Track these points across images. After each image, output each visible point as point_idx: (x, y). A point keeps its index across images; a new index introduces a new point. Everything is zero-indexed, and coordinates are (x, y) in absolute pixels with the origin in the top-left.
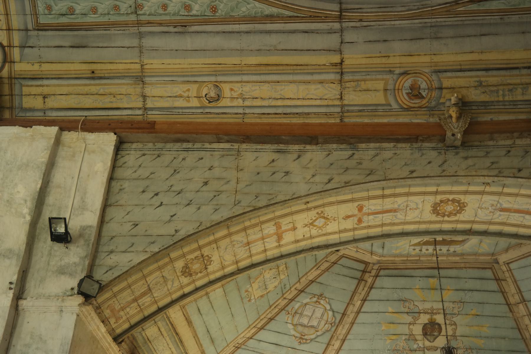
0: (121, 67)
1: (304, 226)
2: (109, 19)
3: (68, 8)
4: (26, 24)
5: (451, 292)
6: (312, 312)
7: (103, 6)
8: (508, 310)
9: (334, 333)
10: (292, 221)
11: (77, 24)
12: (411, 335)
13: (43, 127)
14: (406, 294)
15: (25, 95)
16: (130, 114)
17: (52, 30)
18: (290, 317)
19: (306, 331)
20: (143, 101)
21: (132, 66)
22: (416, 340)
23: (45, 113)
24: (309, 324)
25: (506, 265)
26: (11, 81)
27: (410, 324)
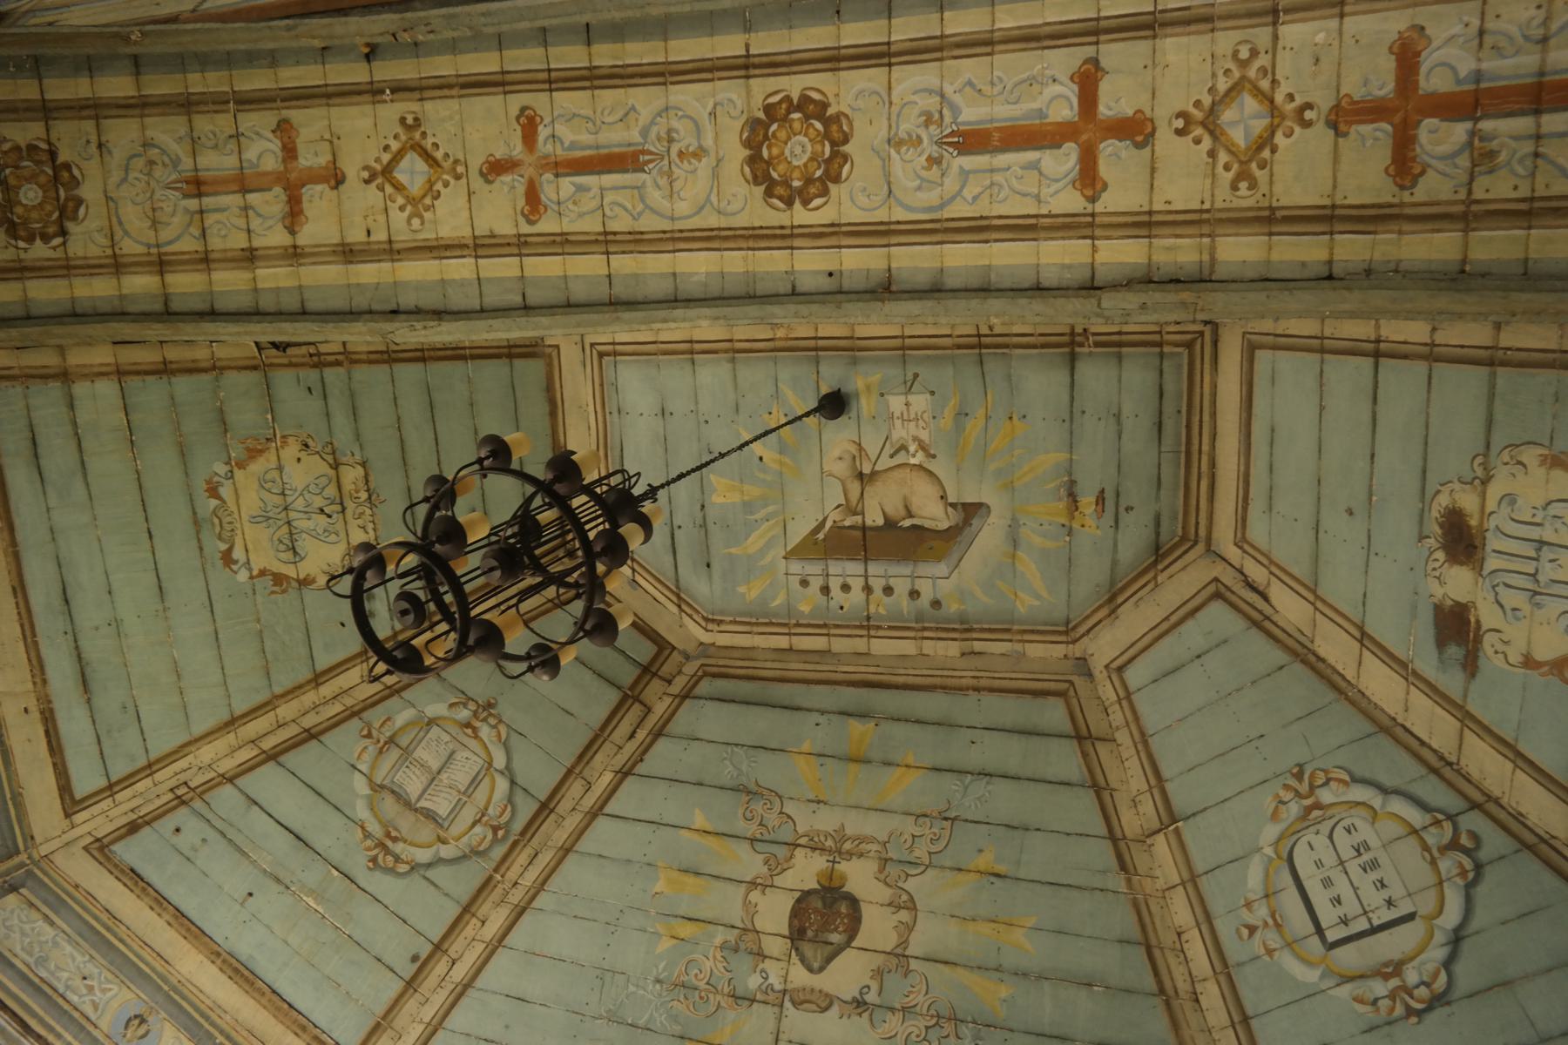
1: (366, 175)
5: (914, 775)
6: (444, 759)
8: (1114, 863)
9: (496, 870)
10: (327, 136)
12: (750, 930)
14: (766, 771)
18: (370, 748)
19: (406, 824)
22: (761, 955)
24: (423, 804)
25: (1115, 677)
27: (753, 884)
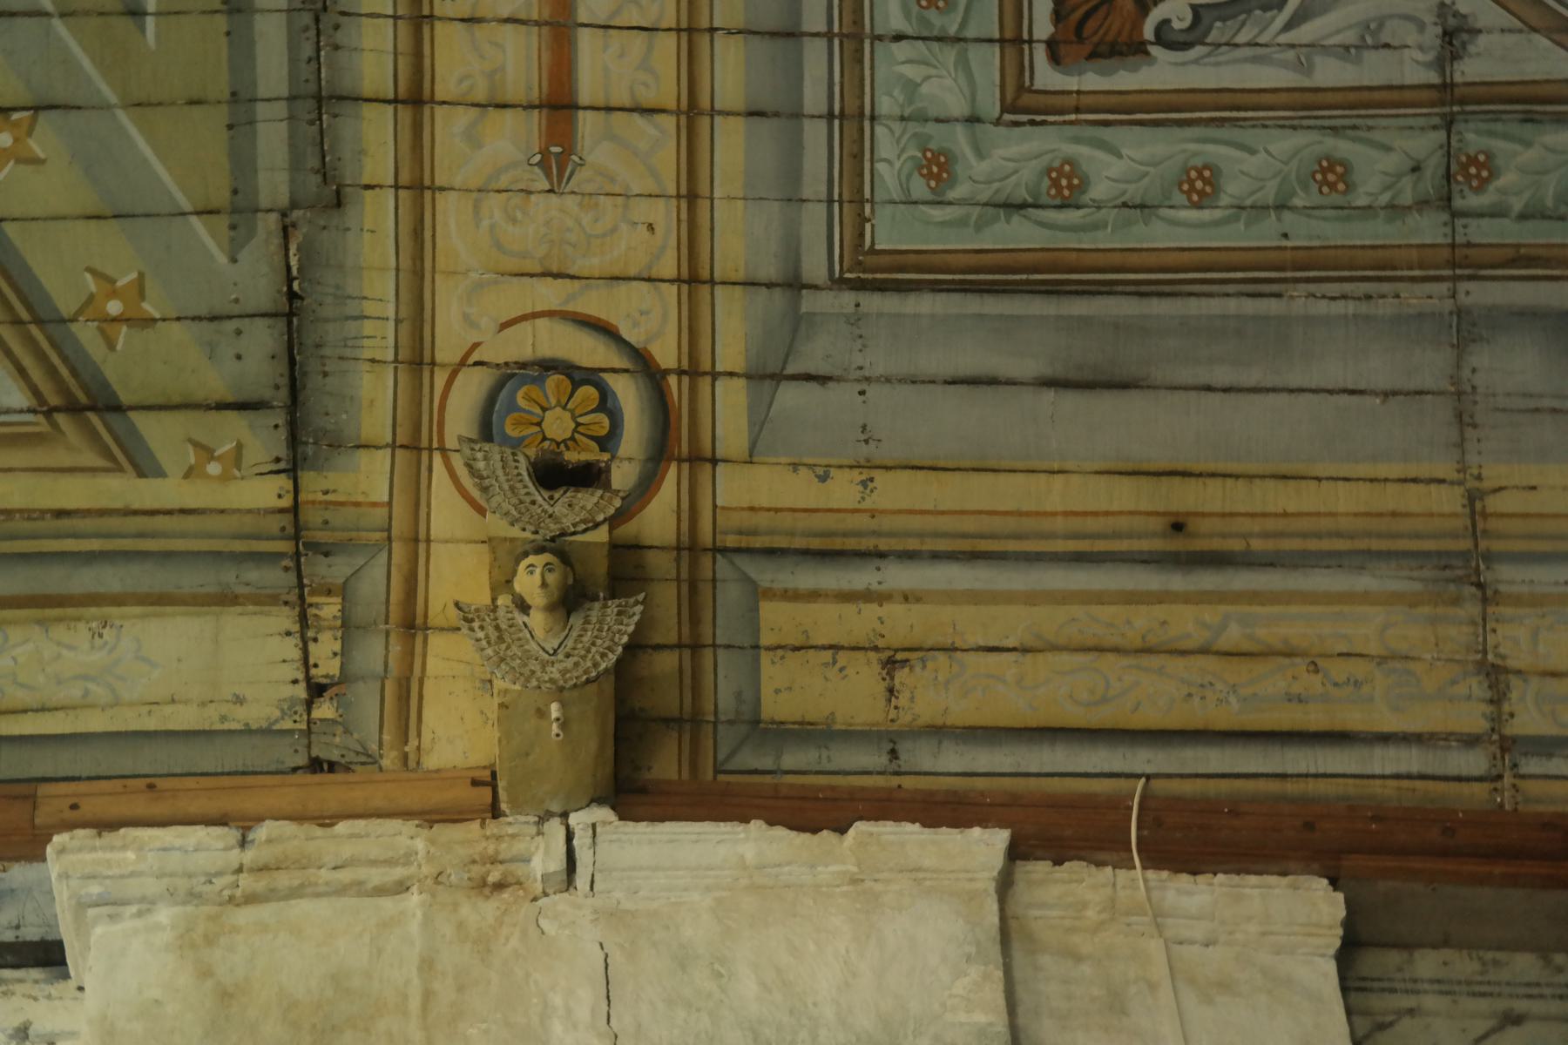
0: (1345, 500)
2: (1285, 236)
3: (1049, 170)
4: (792, 250)
7: (1252, 163)
11: (1088, 259)
13: (917, 827)
15: (768, 649)
16: (1415, 768)
17: (936, 287)
20: (1488, 695)
21: (1413, 499)
23: (893, 754)
26: (694, 565)
